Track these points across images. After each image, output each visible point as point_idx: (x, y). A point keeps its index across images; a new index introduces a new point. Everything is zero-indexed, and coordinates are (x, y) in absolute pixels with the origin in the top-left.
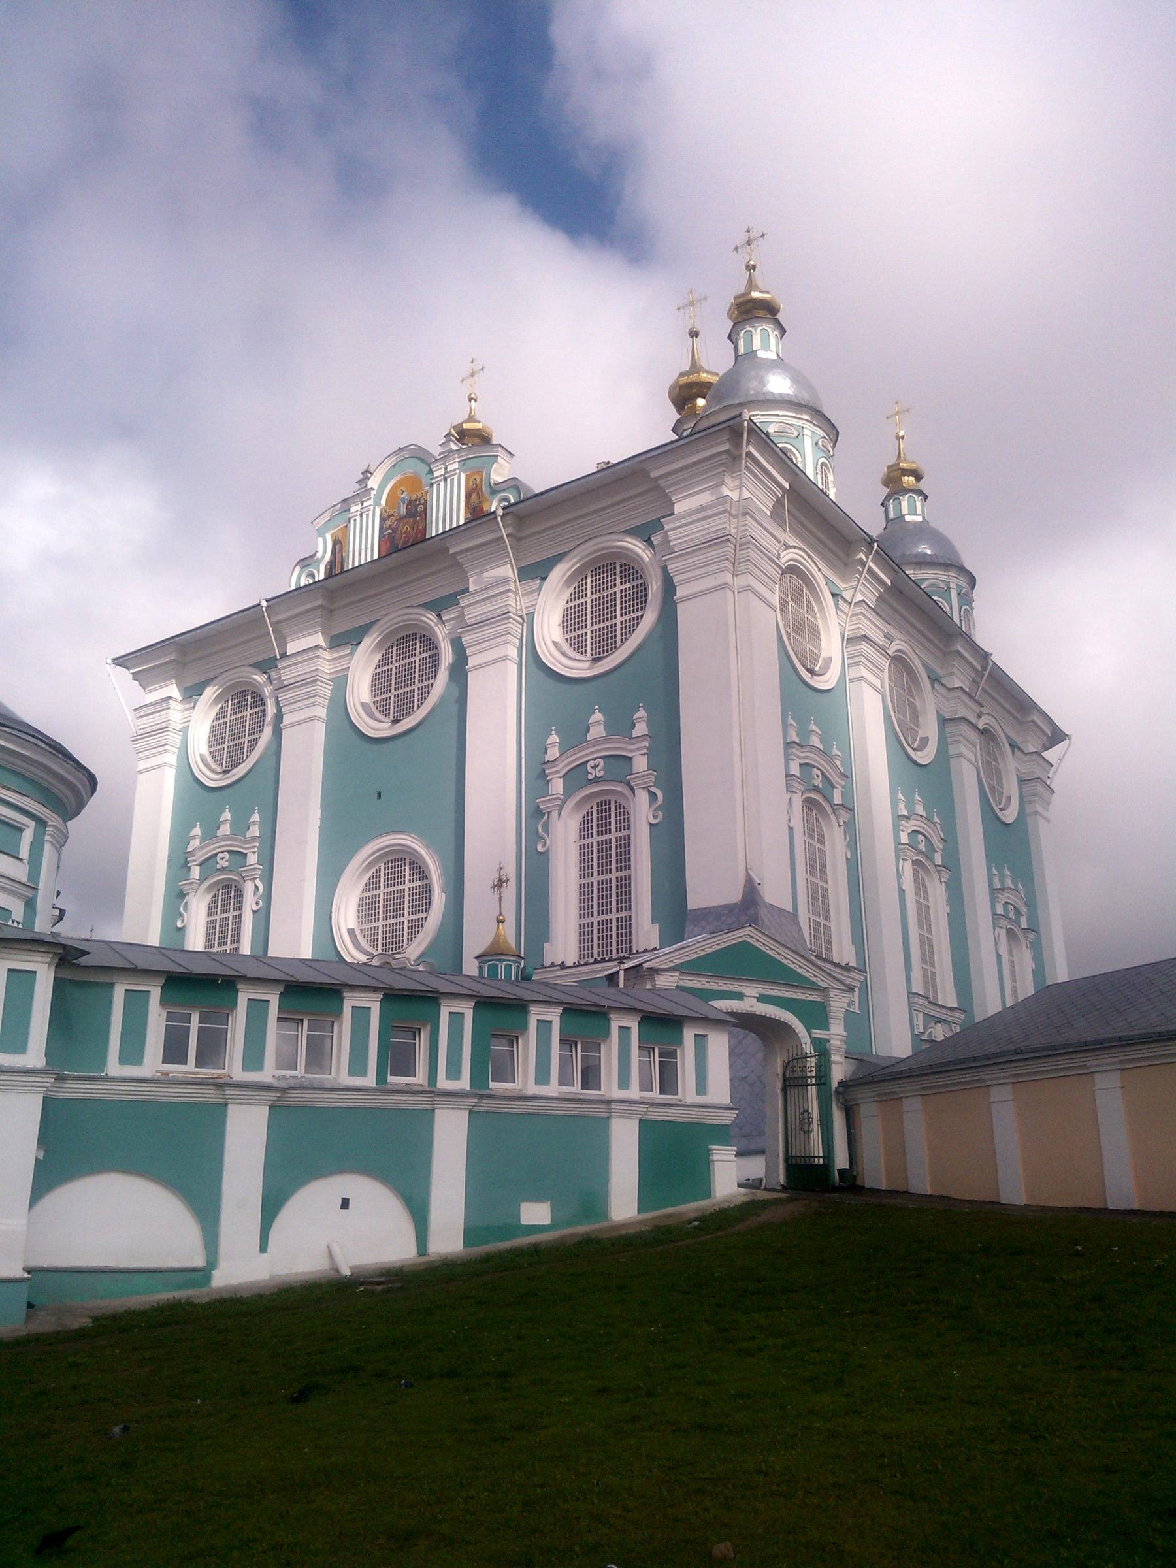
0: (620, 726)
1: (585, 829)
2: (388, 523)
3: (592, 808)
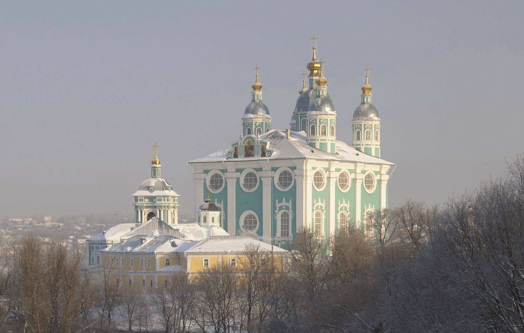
0: (287, 201)
1: (282, 216)
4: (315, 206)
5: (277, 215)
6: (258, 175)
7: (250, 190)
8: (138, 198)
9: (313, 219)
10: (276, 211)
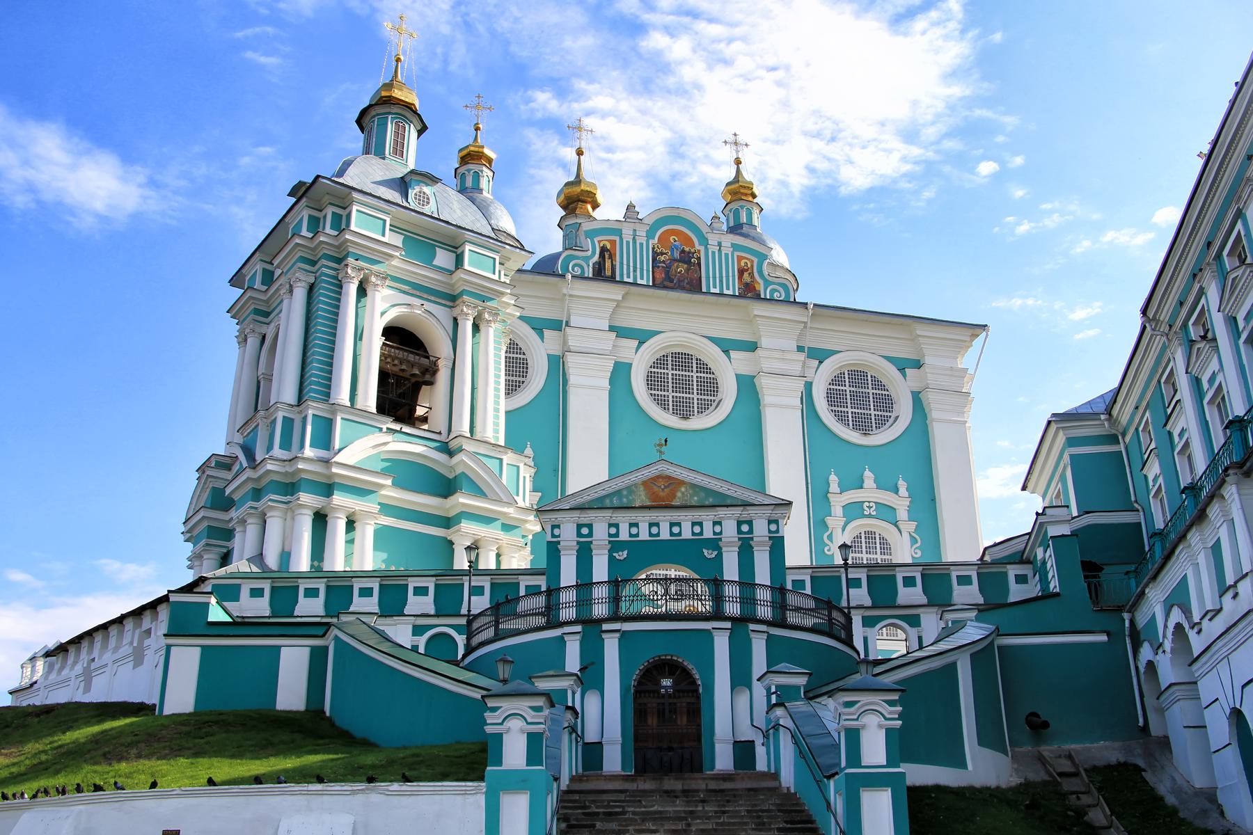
2: (662, 258)
3: (860, 533)
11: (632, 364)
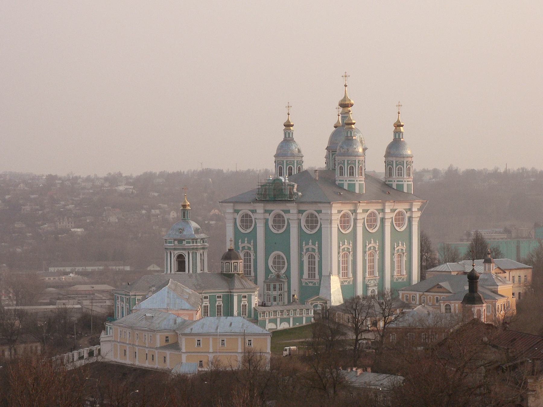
0: (314, 244)
4: (341, 248)
5: (304, 256)
6: (286, 216)
7: (278, 231)
8: (168, 241)
9: (339, 261)
10: (302, 253)
11: (268, 219)
